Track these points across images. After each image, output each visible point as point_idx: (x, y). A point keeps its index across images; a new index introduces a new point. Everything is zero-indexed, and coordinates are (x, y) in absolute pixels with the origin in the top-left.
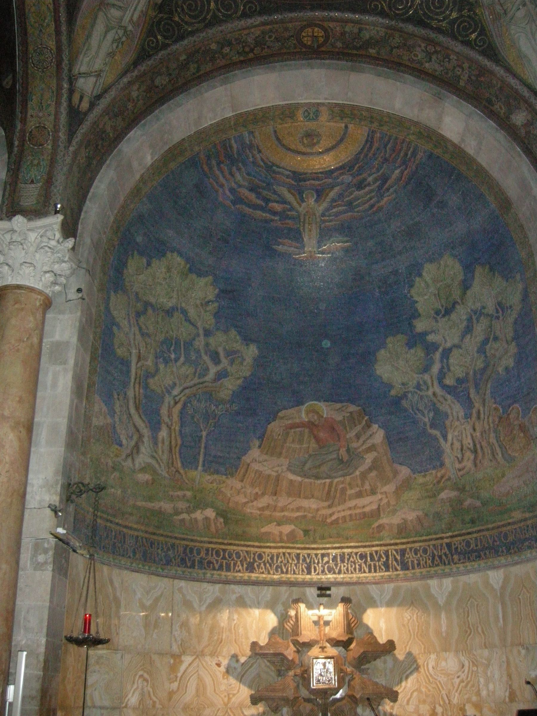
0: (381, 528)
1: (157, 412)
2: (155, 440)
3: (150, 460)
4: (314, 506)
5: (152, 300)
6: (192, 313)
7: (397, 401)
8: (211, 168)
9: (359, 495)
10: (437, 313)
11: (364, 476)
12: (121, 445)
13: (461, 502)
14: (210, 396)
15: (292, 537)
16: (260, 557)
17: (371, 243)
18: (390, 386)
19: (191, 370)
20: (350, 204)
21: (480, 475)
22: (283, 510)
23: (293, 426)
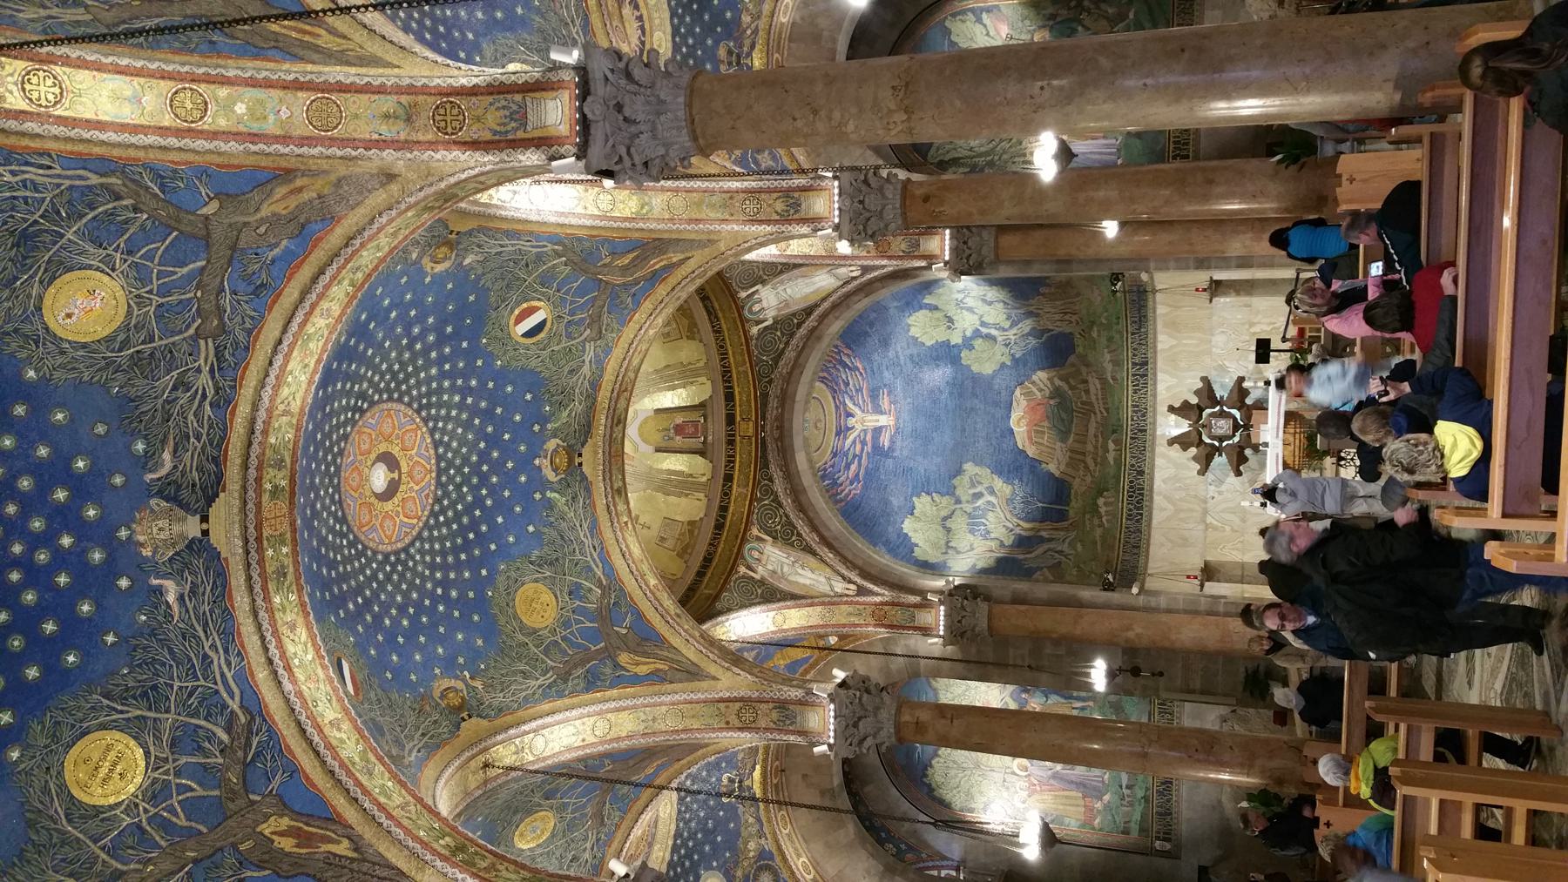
0: (1114, 379)
1: (1028, 538)
2: (1050, 540)
3: (1066, 545)
4: (1094, 425)
5: (943, 542)
6: (944, 513)
7: (1015, 360)
8: (841, 501)
9: (1087, 392)
10: (949, 328)
11: (1072, 388)
12: (1060, 563)
13: (1102, 324)
14: (1010, 501)
15: (1117, 442)
16: (1133, 466)
17: (886, 374)
18: (1003, 365)
19: (990, 514)
20: (857, 391)
21: (1084, 312)
22: (1096, 448)
23: (1030, 438)
